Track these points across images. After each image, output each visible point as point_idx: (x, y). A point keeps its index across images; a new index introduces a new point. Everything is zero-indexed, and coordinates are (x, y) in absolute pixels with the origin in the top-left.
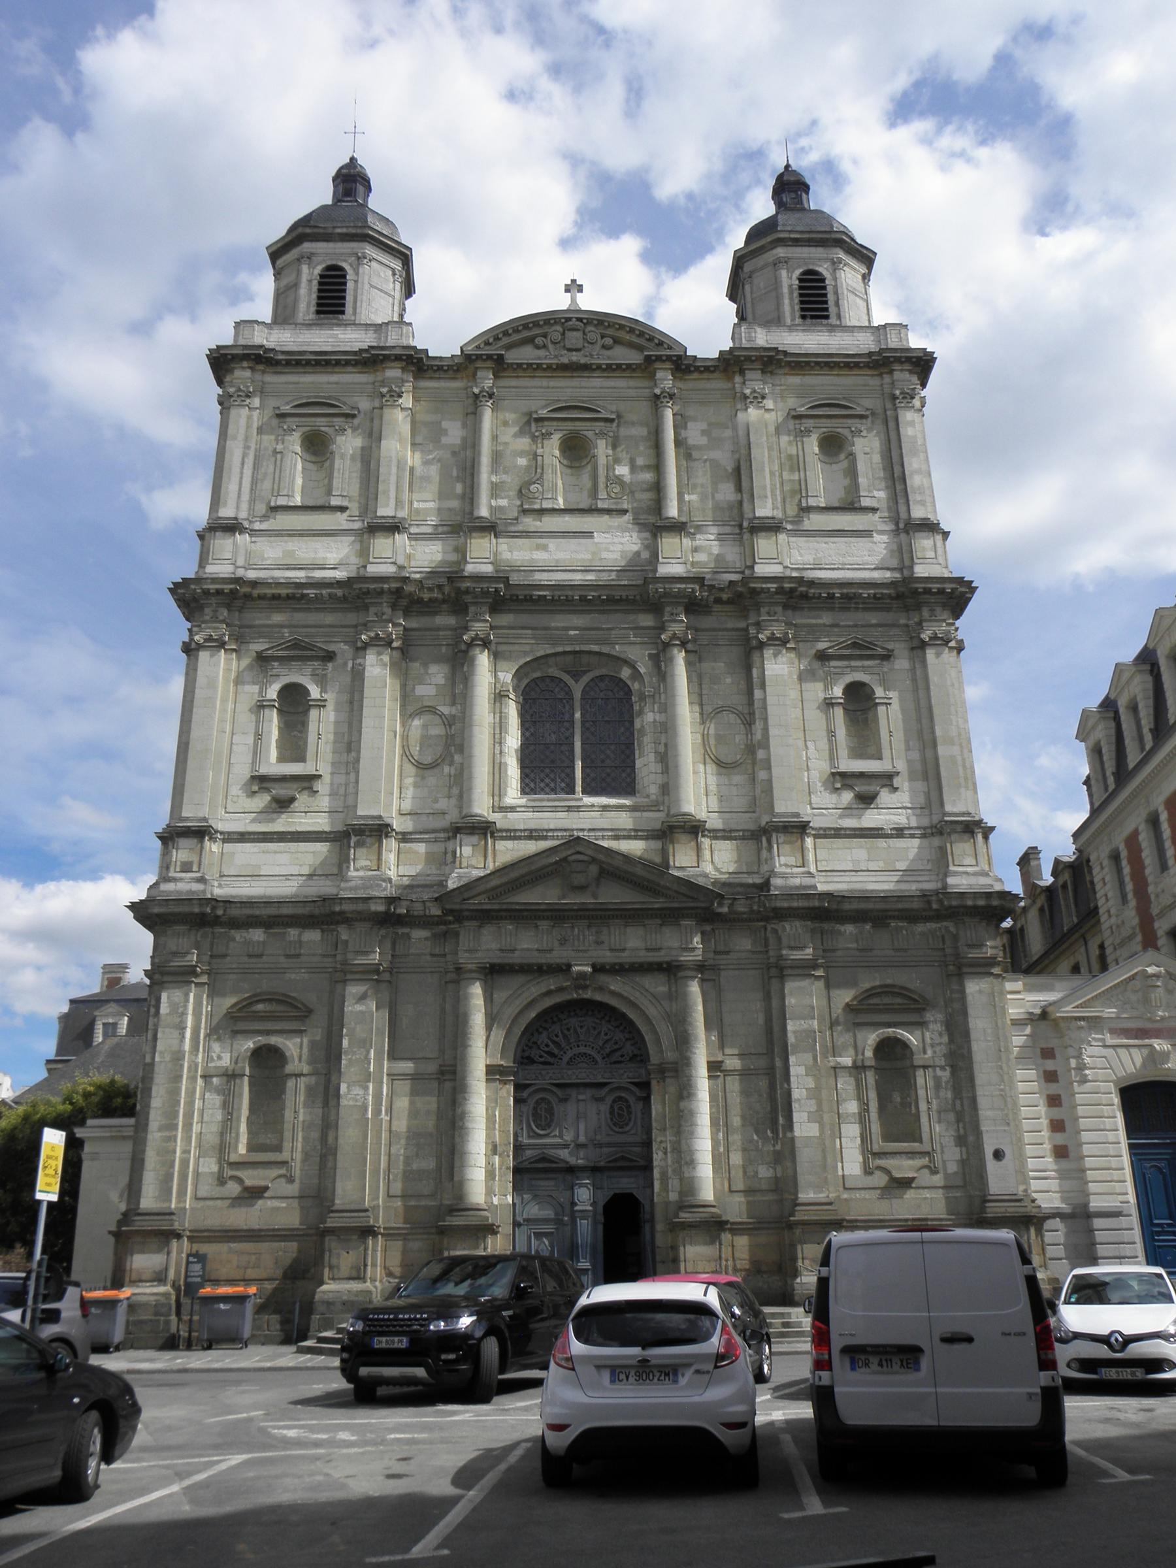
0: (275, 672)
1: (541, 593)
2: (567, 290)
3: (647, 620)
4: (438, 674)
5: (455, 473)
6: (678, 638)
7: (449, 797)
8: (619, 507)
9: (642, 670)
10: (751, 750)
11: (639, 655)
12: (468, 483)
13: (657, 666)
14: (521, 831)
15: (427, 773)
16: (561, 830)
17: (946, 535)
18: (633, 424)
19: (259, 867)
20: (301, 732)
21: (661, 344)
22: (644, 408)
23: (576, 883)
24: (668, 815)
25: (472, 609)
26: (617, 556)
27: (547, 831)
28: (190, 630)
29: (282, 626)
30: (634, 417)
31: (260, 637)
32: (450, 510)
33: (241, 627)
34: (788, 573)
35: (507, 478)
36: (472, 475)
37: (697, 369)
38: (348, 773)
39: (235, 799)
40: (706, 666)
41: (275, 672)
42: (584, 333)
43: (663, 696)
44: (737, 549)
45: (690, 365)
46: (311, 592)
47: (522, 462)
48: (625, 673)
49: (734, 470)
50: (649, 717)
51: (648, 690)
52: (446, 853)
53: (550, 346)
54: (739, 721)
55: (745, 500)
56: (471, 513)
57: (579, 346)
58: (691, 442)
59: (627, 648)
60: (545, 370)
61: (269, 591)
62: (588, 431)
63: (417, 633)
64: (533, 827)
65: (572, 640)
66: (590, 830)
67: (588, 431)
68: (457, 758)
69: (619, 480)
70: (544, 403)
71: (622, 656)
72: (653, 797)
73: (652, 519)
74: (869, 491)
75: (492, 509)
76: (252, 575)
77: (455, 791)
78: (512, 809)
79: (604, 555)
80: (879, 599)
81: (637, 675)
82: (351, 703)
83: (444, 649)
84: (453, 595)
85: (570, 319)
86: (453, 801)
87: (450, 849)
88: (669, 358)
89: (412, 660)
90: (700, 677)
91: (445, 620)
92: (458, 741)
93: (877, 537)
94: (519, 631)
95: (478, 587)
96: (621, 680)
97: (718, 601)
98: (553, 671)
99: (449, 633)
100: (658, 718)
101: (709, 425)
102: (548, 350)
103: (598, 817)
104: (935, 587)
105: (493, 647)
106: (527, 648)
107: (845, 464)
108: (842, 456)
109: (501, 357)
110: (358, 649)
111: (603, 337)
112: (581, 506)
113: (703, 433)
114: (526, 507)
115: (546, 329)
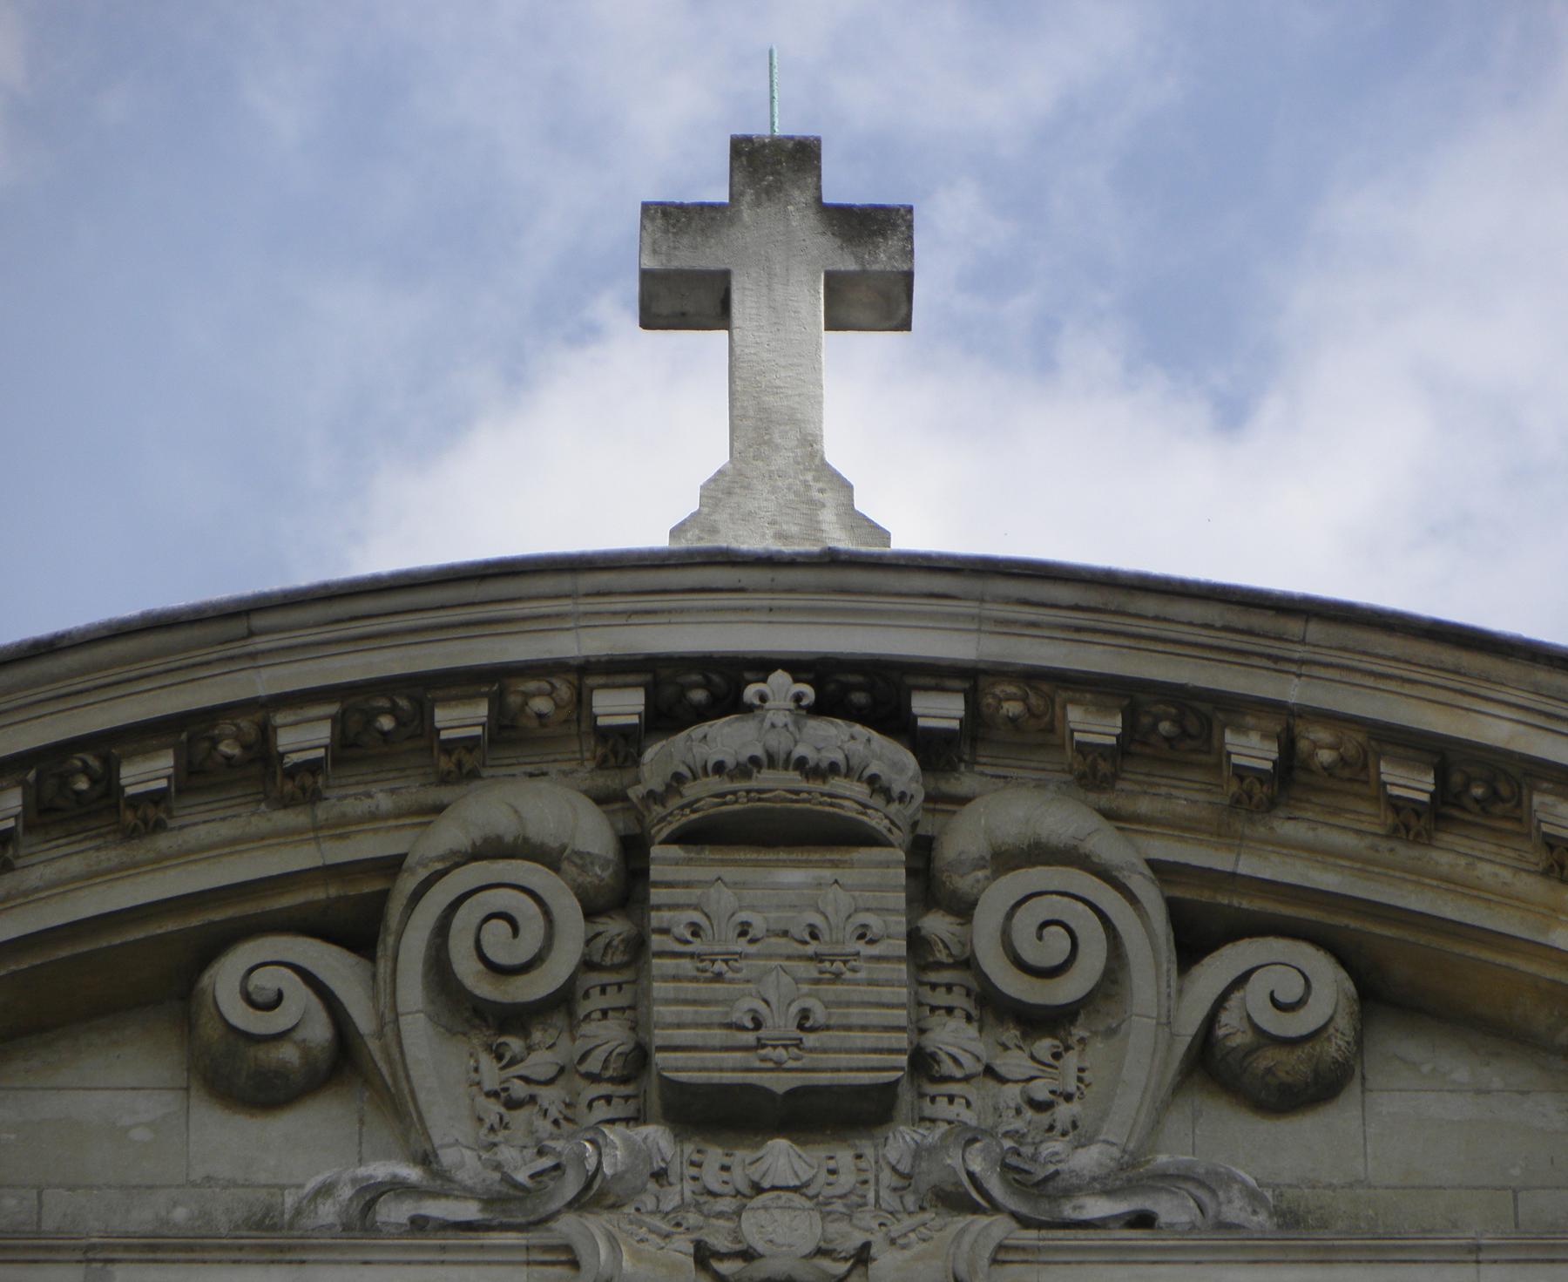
2: (683, 297)
42: (927, 883)
53: (435, 1064)
57: (855, 1058)
85: (724, 684)
102: (396, 1107)
111: (1194, 938)
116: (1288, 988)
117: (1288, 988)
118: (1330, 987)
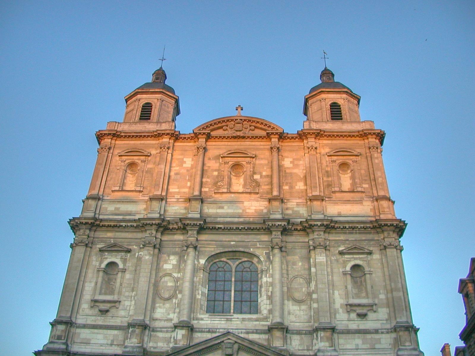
0: (106, 256)
1: (219, 226)
3: (265, 238)
4: (173, 260)
5: (187, 178)
6: (278, 246)
7: (174, 313)
8: (255, 191)
9: (262, 259)
10: (310, 294)
11: (262, 253)
12: (193, 182)
13: (269, 258)
14: (205, 328)
15: (166, 302)
16: (223, 329)
17: (393, 202)
18: (262, 159)
19: (90, 340)
20: (114, 283)
21: (274, 128)
22: (267, 153)
23: (227, 353)
24: (271, 323)
25: (190, 232)
26: (253, 211)
27: (216, 329)
28: (74, 239)
29: (111, 238)
30: (262, 156)
31: (102, 242)
32: (184, 192)
33: (94, 238)
34: (326, 218)
35: (209, 180)
36: (195, 178)
37: (288, 138)
38: (131, 301)
39: (83, 310)
40: (289, 258)
41: (106, 256)
43: (271, 271)
44: (305, 209)
45: (286, 136)
46: (123, 224)
47: (216, 173)
48: (255, 260)
49: (303, 177)
50: (264, 279)
51: (264, 268)
52: (171, 338)
54: (304, 282)
55: (308, 189)
56: (193, 194)
57: (240, 130)
58: (286, 166)
59: (255, 250)
60: (227, 138)
61: (107, 224)
62: (243, 161)
63: (167, 242)
64: (210, 327)
65: (231, 246)
66: (236, 329)
67: (243, 161)
68: (180, 296)
69: (256, 181)
70: (226, 151)
71: (253, 253)
72: (265, 315)
73: (270, 196)
74: (360, 185)
75: (201, 192)
76: (101, 217)
77: (177, 310)
78: (202, 319)
79: (248, 211)
80: (365, 229)
81: (260, 261)
82: (136, 271)
83: (177, 249)
84: (182, 227)
85: (237, 119)
86: (176, 315)
87: (172, 337)
88: (277, 133)
89: (163, 254)
90: (287, 262)
91: (179, 237)
92: (180, 288)
93: (365, 203)
94: (210, 242)
95: (192, 223)
96: (253, 263)
97: (296, 230)
98: (224, 259)
99: (180, 242)
100: (268, 280)
101: (294, 159)
103: (238, 323)
104: (389, 223)
105: (198, 248)
106: (213, 249)
107: (350, 175)
108: (349, 171)
109: (209, 133)
110: (141, 248)
111: (250, 126)
112: (239, 191)
113: (291, 162)
114: (216, 191)
115: (228, 123)
116: (253, 128)
117: (253, 128)
118: (254, 127)
